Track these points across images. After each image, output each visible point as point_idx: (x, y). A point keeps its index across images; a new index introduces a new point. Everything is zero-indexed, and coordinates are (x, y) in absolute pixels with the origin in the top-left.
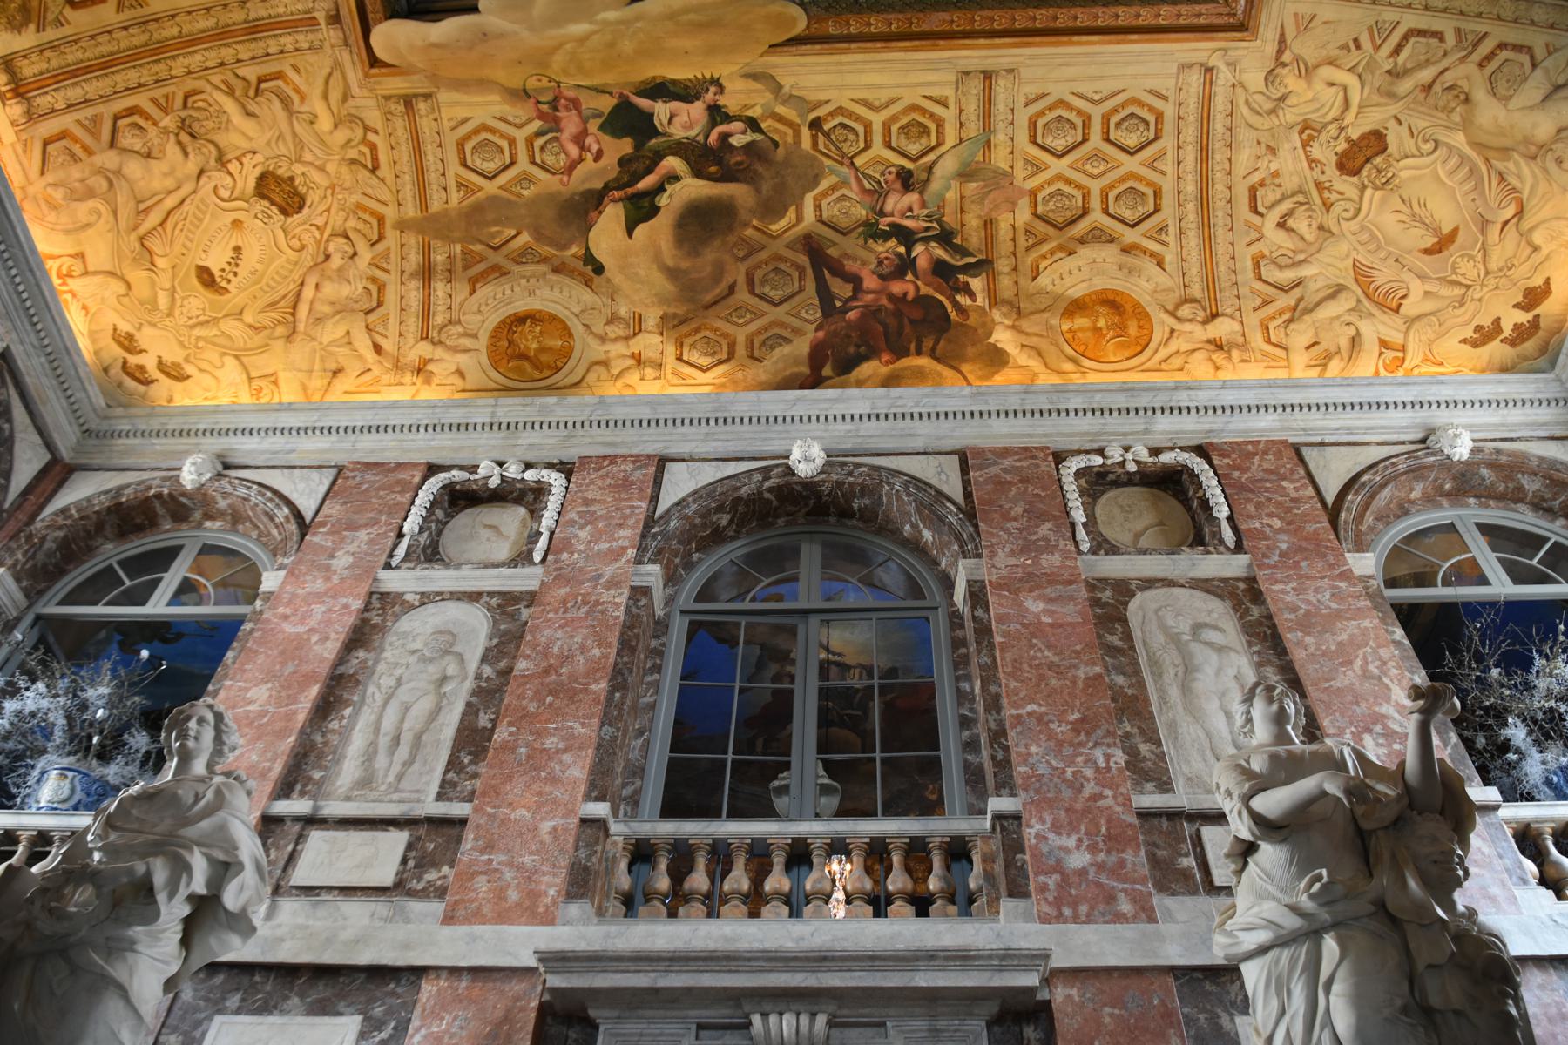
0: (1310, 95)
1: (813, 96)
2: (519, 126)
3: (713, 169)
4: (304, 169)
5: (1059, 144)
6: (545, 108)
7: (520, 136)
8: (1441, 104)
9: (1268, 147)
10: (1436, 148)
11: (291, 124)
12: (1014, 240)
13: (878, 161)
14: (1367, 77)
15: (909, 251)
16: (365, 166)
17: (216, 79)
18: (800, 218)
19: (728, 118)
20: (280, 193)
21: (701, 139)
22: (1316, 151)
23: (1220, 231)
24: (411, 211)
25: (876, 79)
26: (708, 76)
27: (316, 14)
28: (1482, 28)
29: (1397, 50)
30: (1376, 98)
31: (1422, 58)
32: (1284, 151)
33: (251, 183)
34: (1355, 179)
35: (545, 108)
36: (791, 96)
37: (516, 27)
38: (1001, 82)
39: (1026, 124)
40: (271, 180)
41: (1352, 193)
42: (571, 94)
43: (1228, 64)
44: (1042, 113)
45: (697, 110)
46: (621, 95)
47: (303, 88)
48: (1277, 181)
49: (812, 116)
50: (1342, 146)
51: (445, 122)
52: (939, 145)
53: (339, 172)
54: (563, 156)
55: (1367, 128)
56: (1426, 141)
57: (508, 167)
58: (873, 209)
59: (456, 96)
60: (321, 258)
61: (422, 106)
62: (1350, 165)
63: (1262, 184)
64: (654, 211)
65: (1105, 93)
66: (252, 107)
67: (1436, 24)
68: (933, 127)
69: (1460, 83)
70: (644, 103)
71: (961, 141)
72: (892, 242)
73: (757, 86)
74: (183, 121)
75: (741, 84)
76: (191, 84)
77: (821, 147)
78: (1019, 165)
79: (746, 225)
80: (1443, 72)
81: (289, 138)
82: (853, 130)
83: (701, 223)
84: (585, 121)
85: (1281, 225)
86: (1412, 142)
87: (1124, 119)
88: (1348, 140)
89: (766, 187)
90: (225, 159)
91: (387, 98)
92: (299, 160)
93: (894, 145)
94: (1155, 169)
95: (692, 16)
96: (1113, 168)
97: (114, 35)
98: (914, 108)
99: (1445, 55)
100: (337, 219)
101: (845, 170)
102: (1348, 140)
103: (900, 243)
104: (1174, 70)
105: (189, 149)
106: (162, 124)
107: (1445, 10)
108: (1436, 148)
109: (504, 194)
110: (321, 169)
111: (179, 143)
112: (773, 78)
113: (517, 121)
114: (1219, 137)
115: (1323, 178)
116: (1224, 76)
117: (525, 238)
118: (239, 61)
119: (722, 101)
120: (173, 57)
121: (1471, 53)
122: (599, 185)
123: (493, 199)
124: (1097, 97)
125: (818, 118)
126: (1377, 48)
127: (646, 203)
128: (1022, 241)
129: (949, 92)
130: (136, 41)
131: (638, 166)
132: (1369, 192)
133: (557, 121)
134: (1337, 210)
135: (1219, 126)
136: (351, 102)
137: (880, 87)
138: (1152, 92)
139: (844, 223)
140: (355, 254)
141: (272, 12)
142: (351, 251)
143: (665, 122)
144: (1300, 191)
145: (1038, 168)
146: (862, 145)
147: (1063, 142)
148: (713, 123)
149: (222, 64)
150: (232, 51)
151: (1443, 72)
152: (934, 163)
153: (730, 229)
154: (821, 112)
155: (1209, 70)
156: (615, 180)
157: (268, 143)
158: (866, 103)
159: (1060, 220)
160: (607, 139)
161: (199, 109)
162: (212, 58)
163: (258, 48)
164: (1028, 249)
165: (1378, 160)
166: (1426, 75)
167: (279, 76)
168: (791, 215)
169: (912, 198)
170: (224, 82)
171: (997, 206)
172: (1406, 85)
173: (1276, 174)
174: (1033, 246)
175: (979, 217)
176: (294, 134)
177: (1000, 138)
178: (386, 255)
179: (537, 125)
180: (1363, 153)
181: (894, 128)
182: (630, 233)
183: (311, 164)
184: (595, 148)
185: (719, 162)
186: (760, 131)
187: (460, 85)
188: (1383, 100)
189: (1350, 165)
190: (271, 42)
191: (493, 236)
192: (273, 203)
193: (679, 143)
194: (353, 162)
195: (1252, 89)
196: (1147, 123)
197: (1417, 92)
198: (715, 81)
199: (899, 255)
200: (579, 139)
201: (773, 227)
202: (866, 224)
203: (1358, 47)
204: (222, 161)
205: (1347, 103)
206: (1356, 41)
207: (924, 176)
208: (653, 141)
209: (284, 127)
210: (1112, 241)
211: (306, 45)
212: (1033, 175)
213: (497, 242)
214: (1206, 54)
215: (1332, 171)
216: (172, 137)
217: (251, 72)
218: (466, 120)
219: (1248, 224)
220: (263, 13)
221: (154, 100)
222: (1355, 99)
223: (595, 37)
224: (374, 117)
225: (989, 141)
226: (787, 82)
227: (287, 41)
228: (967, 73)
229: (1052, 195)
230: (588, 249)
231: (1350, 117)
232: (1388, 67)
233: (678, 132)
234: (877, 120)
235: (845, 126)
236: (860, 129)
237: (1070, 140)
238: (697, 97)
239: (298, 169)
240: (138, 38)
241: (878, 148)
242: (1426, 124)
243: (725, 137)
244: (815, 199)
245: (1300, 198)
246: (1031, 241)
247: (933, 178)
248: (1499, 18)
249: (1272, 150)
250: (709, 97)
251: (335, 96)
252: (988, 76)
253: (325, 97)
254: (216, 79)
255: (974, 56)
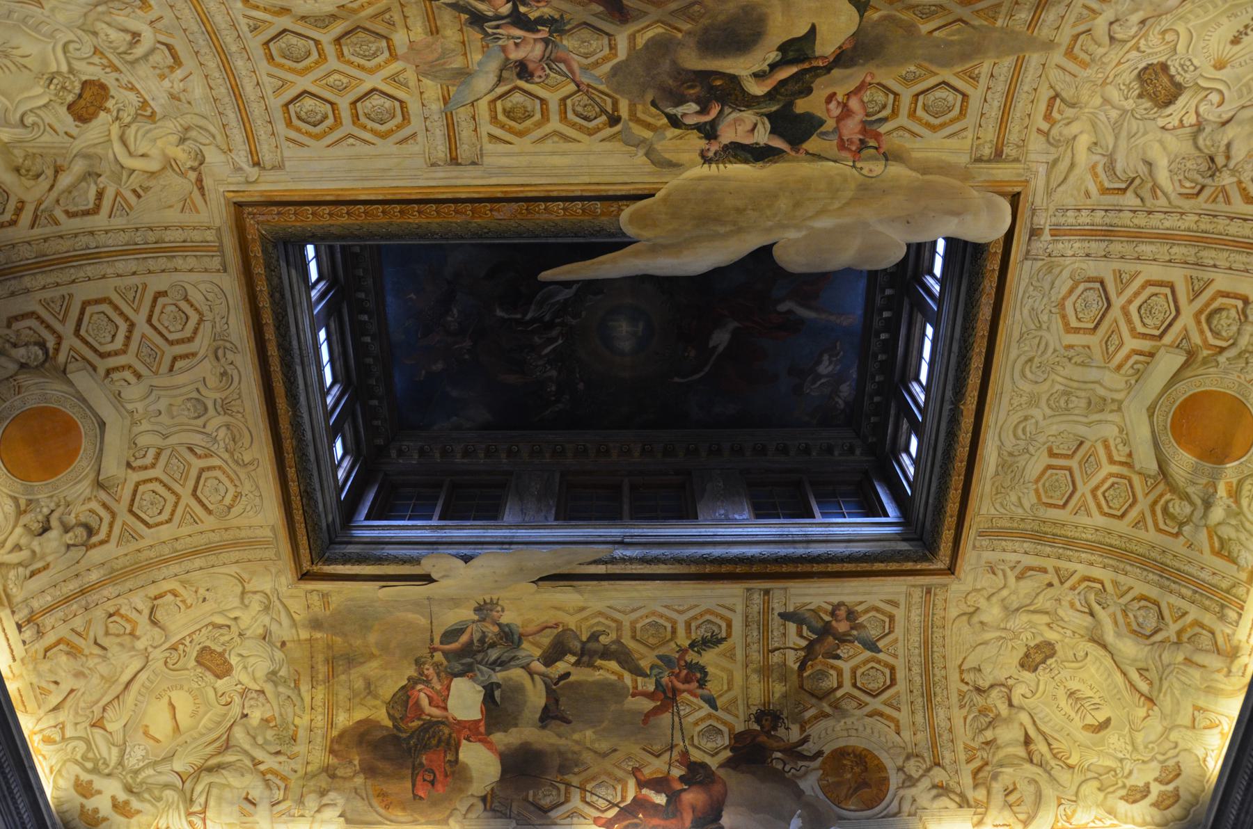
0: (159, 143)
1: (616, 145)
2: (902, 128)
3: (718, 83)
4: (1125, 103)
5: (377, 100)
6: (872, 143)
7: (903, 120)
8: (39, 160)
9: (179, 100)
10: (22, 120)
11: (1115, 146)
12: (405, 17)
13: (553, 88)
14: (117, 168)
15: (515, 8)
16: (1063, 100)
17: (1162, 201)
18: (632, 38)
19: (698, 127)
20: (1160, 86)
21: (727, 110)
22: (132, 96)
23: (195, 28)
24: (1035, 59)
25: (557, 160)
26: (713, 166)
27: (1049, 238)
28: (37, 231)
29: (100, 195)
30: (99, 150)
31: (75, 193)
32: (163, 99)
33: (1181, 101)
34: (84, 78)
35: (872, 143)
36: (637, 146)
37: (880, 228)
38: (441, 155)
39: (412, 119)
40: (1162, 98)
41: (77, 65)
42: (845, 154)
43: (241, 169)
44: (399, 127)
45: (728, 135)
46: (797, 152)
47: (1089, 177)
48: (158, 71)
49: (618, 128)
50: (110, 104)
51: (970, 136)
52: (494, 101)
53: (1091, 96)
54: (866, 99)
55: (94, 123)
56: (34, 124)
57: (922, 92)
58: (555, 45)
59: (952, 159)
60: (1148, 23)
61: (987, 151)
62: (95, 89)
63: (172, 69)
64: (783, 48)
65: (344, 144)
66: (1143, 170)
67: (77, 223)
68: (501, 117)
69: (32, 182)
70: (778, 143)
71: (472, 104)
72: (533, 15)
73: (667, 156)
74: (1212, 176)
75: (684, 157)
76: (1187, 204)
77: (609, 101)
78: (412, 82)
79: (689, 33)
80: (52, 187)
81: (1124, 134)
82: (578, 115)
83: (738, 35)
84: (837, 130)
85: (136, 35)
86: (47, 120)
87: (322, 122)
88: (108, 111)
89: (666, 65)
90: (1195, 129)
91: (1017, 160)
92: (1125, 112)
93: (538, 102)
94: (280, 79)
95: (722, 230)
96: (320, 79)
97: (1228, 265)
98: (520, 134)
99: (58, 201)
100: (1114, 55)
101: (585, 80)
102: (108, 111)
103: (525, 15)
104: (287, 164)
105: (1222, 148)
106: (1235, 179)
107: (76, 235)
108: (22, 120)
109: (934, 68)
110: (1106, 101)
111: (1228, 158)
112: (653, 163)
113: (901, 133)
114: (229, 107)
115: (115, 75)
116: (242, 159)
117: (925, 28)
118: (1134, 212)
119: (703, 144)
120: (1189, 230)
121: (36, 209)
122: (836, 72)
123: (946, 63)
124: (351, 141)
125: (611, 126)
126: (117, 194)
127: (791, 55)
128: (397, 17)
129: (489, 147)
130: (1213, 254)
131: (792, 87)
132: (64, 68)
133: (864, 131)
134: (87, 50)
135: (232, 117)
136: (1051, 158)
137: (553, 153)
138: (302, 145)
139: (586, 33)
140: (1111, 23)
141: (1086, 244)
142: (1116, 27)
143: (760, 126)
144: (132, 63)
145: (394, 78)
146: (569, 102)
147: (375, 103)
148: (713, 124)
149: (1150, 213)
150: (1136, 221)
151: (52, 187)
152: (497, 85)
153: (706, 30)
154: (609, 131)
155: (256, 164)
156: (818, 76)
157: (1145, 133)
158: (566, 138)
159: (361, 35)
160: (819, 112)
161: (1192, 181)
162: (1155, 220)
163: (1112, 218)
164: (389, 9)
165: (70, 98)
166: (65, 180)
167: (1105, 191)
168: (641, 41)
169: (515, 55)
170: (1155, 197)
171: (428, 46)
172: (79, 167)
173: (162, 77)
174: (383, 13)
175: (444, 37)
176: (1116, 138)
177: (436, 107)
178: (1080, 19)
179: (883, 129)
180: (88, 102)
181: (538, 116)
182: (813, 29)
183: (1114, 107)
184: (833, 105)
185: (712, 88)
186: (669, 116)
187: (944, 169)
188: (92, 150)
189: (95, 89)
190: (1098, 220)
191: (958, 31)
192: (1171, 78)
193: (749, 106)
194: (1073, 106)
195: (212, 148)
196: (299, 118)
197: (66, 164)
198: (706, 160)
199: (525, 4)
200: (846, 112)
201: (660, 30)
202: (562, 32)
203: (134, 191)
204: (1199, 127)
205: (124, 143)
206: (139, 196)
207: (505, 74)
208: (774, 109)
209: (1123, 144)
210: (303, 18)
211: (1069, 213)
212: (398, 74)
213: (955, 27)
214: (261, 179)
215: (109, 79)
216: (1231, 165)
217: (1130, 199)
218: (949, 137)
219: (171, 35)
220: (1093, 245)
221: (1228, 201)
222: (118, 147)
223: (809, 214)
224: (1036, 144)
225: (445, 104)
226: (640, 158)
227: (1084, 218)
228: (474, 163)
229: (375, 55)
230: (861, 16)
231: (115, 130)
232: (100, 179)
233: (749, 116)
234: (555, 124)
235: (586, 118)
236: (570, 115)
237: (367, 103)
238: (726, 148)
239: (1129, 104)
240: (1208, 256)
241: (553, 98)
242: (43, 139)
243: (704, 111)
244: (616, 55)
245: (129, 58)
246: (387, 16)
247: (497, 72)
248: (29, 243)
249: (173, 97)
250: (715, 147)
251: (1063, 166)
252: (454, 161)
253: (1072, 165)
254: (1162, 201)
255: (468, 181)
